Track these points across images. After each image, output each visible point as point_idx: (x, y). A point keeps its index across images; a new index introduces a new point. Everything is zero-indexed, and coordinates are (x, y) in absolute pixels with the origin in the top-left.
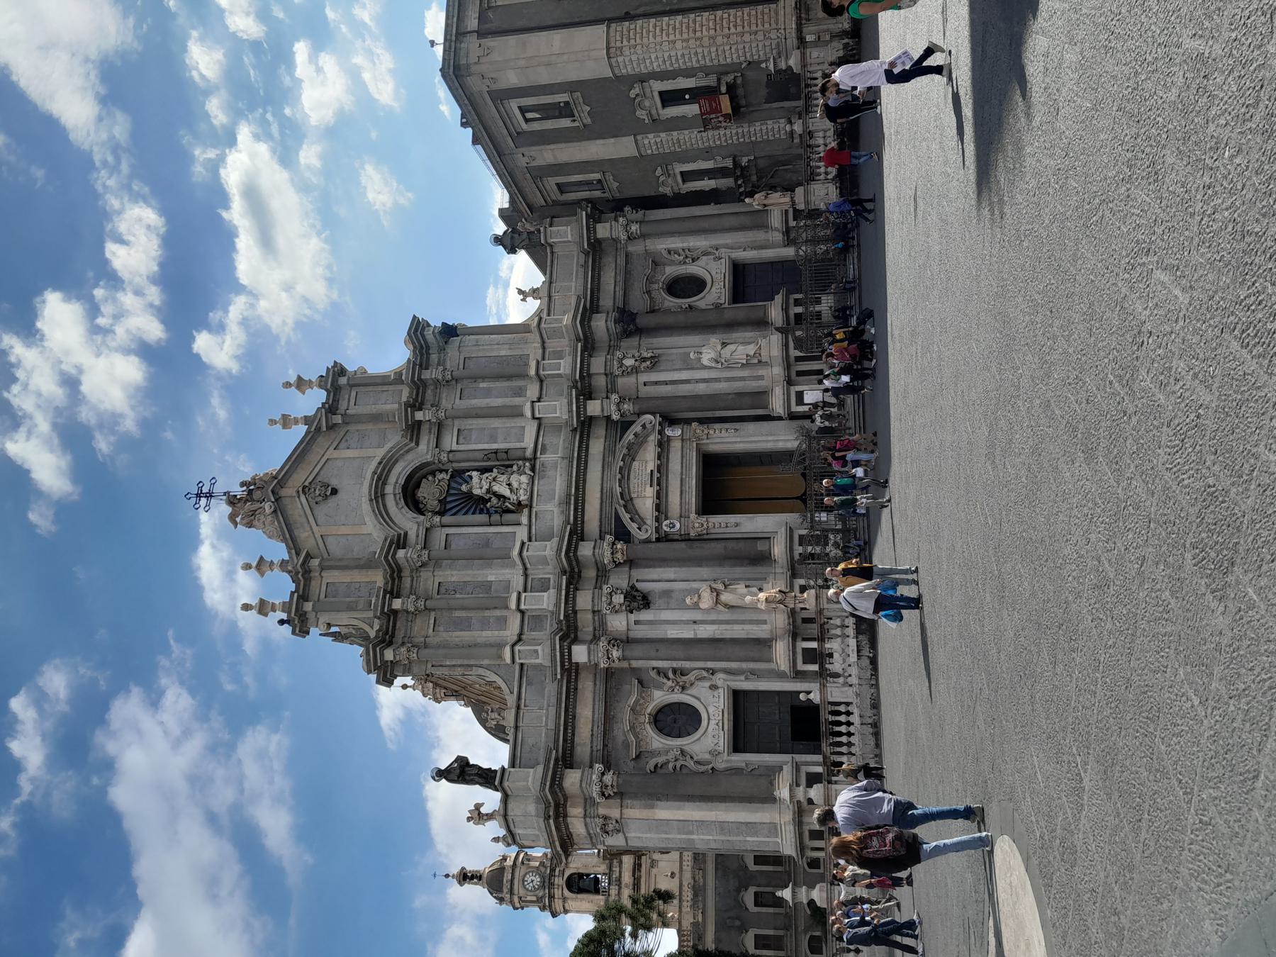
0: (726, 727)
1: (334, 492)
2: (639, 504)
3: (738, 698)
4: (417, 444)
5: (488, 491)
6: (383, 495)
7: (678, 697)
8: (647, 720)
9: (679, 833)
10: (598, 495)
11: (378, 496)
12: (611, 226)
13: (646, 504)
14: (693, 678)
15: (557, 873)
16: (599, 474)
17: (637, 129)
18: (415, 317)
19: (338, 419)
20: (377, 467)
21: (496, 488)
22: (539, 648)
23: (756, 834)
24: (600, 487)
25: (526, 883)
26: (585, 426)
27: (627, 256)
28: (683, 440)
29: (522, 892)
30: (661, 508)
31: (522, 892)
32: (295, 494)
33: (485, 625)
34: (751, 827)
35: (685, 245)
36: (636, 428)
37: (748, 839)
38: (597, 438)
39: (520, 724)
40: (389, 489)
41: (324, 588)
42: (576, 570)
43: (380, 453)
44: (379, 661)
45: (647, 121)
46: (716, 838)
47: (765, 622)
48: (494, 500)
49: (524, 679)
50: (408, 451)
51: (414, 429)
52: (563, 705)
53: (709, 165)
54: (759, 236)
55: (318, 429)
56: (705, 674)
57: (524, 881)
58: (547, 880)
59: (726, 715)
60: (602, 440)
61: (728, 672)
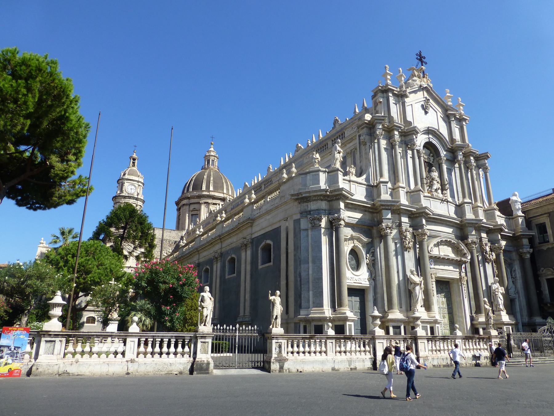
1: (426, 113)
8: (356, 245)
11: (429, 131)
12: (527, 245)
14: (371, 269)
15: (134, 200)
21: (435, 182)
23: (315, 296)
25: (131, 186)
32: (425, 96)
35: (518, 278)
36: (466, 251)
39: (351, 183)
40: (430, 136)
42: (413, 216)
44: (378, 121)
46: (310, 276)
51: (453, 152)
54: (525, 312)
56: (373, 276)
57: (132, 185)
58: (132, 196)
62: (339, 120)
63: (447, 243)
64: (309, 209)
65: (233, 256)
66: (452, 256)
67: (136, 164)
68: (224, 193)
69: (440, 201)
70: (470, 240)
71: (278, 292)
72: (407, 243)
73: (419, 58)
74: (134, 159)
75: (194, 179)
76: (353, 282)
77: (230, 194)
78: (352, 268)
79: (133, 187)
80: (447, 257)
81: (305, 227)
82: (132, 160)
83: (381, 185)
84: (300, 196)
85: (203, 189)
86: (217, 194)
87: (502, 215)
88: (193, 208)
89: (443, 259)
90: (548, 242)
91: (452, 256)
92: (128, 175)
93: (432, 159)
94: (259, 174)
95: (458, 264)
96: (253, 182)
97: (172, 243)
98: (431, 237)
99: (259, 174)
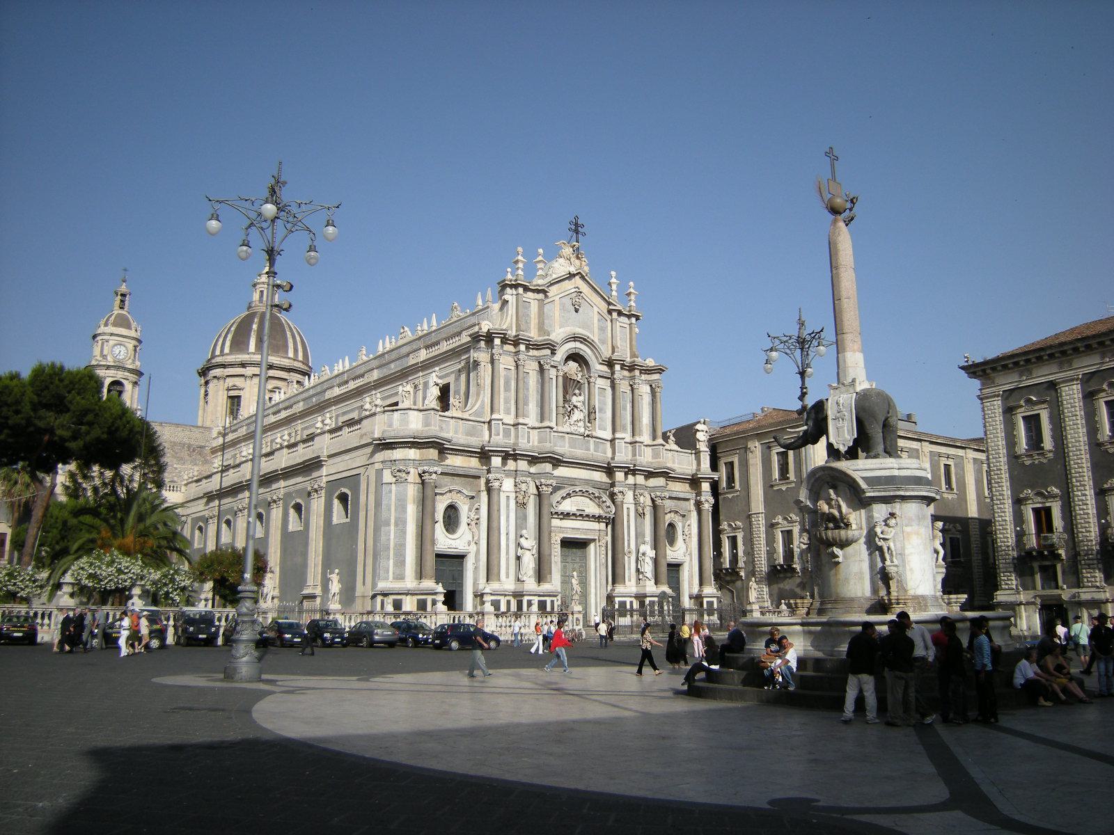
0: (449, 550)
1: (577, 311)
2: (568, 501)
3: (461, 557)
4: (601, 364)
5: (575, 406)
6: (575, 341)
7: (464, 519)
9: (396, 518)
10: (573, 477)
11: (575, 338)
13: (568, 506)
16: (583, 478)
17: (770, 514)
18: (667, 369)
19: (615, 315)
20: (591, 339)
22: (501, 436)
23: (395, 565)
24: (576, 477)
26: (609, 470)
27: (688, 500)
28: (599, 530)
29: (111, 343)
30: (566, 516)
31: (111, 343)
33: (507, 401)
34: (401, 563)
36: (609, 503)
37: (391, 562)
38: (601, 477)
40: (578, 345)
41: (528, 300)
43: (595, 338)
45: (774, 521)
47: (507, 576)
48: (569, 409)
49: (476, 423)
50: (597, 357)
51: (610, 364)
52: (466, 449)
53: (741, 553)
55: (609, 304)
57: (121, 345)
58: (121, 365)
59: (456, 550)
60: (600, 480)
61: (478, 552)
62: (459, 308)
63: (583, 493)
64: (394, 458)
65: (299, 501)
66: (592, 508)
67: (127, 303)
68: (289, 358)
69: (582, 437)
70: (616, 490)
71: (337, 571)
72: (521, 498)
73: (573, 227)
74: (123, 295)
75: (233, 329)
76: (446, 547)
77: (300, 358)
78: (447, 530)
79: (123, 348)
80: (578, 513)
81: (390, 481)
82: (119, 297)
83: (493, 422)
84: (383, 441)
85: (250, 351)
86: (274, 360)
87: (679, 449)
88: (231, 384)
89: (574, 515)
90: (734, 487)
91: (592, 508)
92: (115, 325)
93: (580, 375)
94: (347, 358)
95: (598, 519)
96: (336, 368)
97: (194, 451)
98: (556, 489)
99: (347, 358)
